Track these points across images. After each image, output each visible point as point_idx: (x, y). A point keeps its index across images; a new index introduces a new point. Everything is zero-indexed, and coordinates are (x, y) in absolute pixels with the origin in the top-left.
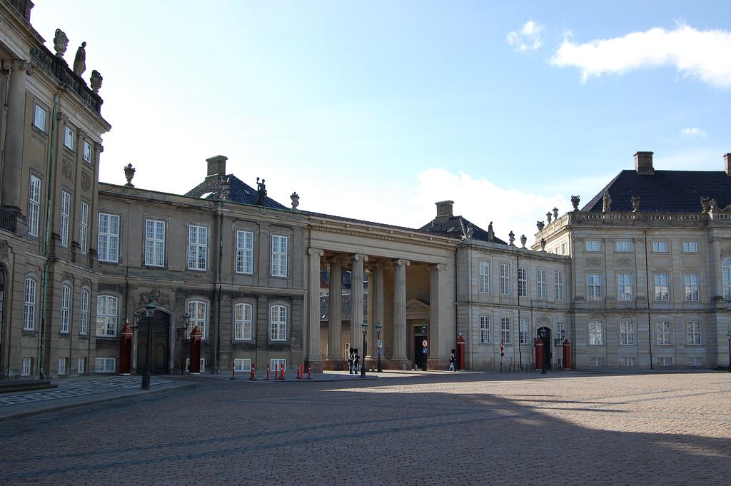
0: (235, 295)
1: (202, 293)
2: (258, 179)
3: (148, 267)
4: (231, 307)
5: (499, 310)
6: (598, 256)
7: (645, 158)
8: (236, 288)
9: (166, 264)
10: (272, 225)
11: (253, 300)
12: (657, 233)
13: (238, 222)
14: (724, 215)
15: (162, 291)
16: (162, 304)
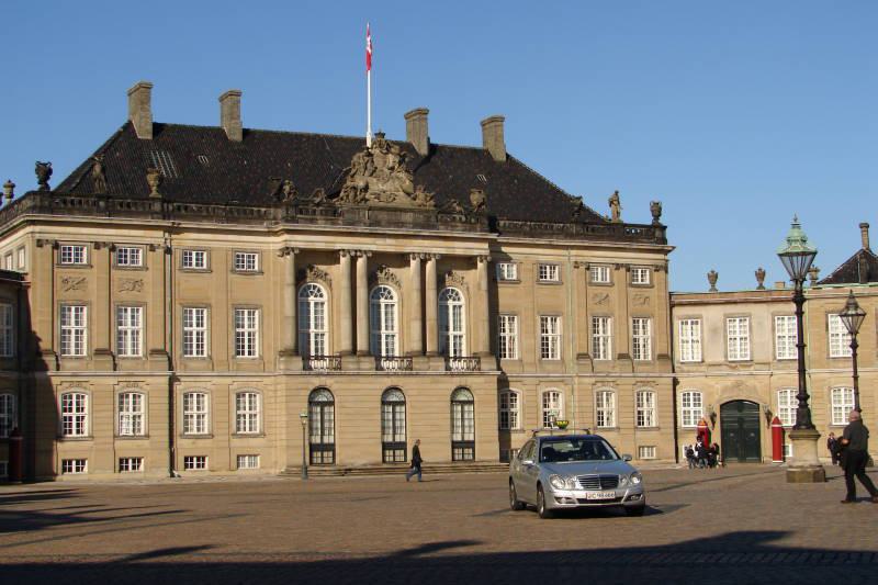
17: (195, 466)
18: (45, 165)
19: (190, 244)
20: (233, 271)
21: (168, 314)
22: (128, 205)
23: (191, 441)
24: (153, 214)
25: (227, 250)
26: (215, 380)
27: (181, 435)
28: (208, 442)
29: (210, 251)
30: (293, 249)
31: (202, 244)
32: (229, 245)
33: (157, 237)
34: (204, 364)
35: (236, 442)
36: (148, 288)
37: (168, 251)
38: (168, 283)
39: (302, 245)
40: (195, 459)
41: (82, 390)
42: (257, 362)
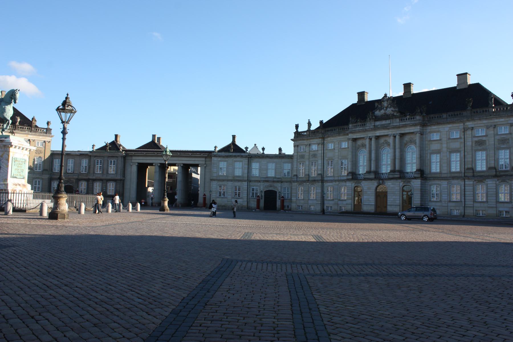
0: (95, 180)
1: (85, 180)
2: (105, 142)
3: (68, 173)
4: (93, 184)
5: (232, 182)
6: (304, 153)
7: (361, 95)
8: (94, 178)
9: (74, 172)
10: (109, 157)
11: (101, 181)
12: (329, 139)
13: (97, 157)
14: (355, 125)
15: (71, 179)
16: (71, 183)
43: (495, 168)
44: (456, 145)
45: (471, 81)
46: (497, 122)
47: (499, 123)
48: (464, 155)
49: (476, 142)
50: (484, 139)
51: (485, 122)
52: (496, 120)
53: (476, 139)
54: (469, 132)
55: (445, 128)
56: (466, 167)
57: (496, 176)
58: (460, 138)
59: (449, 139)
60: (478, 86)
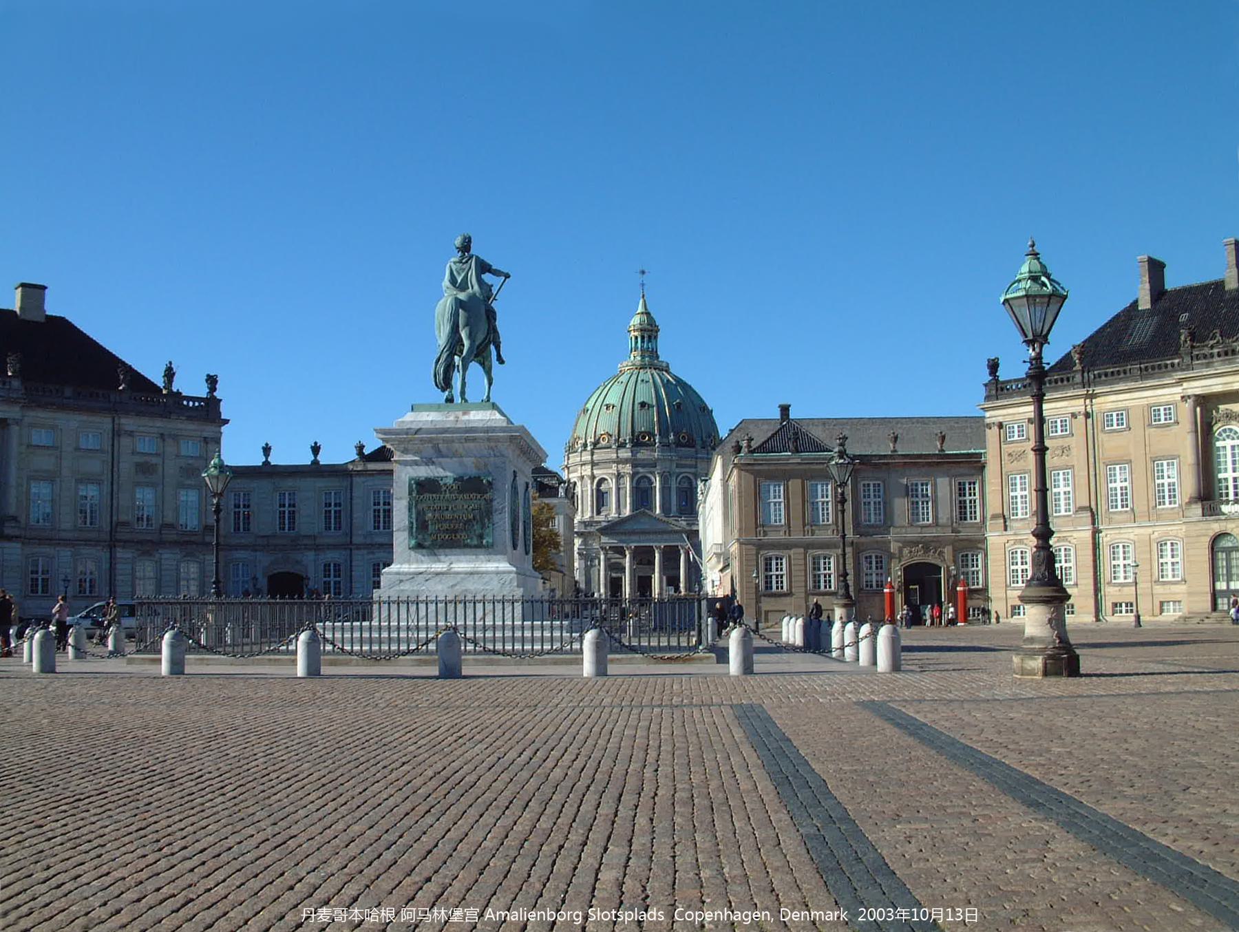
17: (1124, 611)
18: (993, 360)
19: (1110, 406)
20: (1150, 425)
21: (1092, 473)
22: (1056, 381)
23: (1117, 589)
24: (1074, 386)
25: (1143, 406)
26: (1137, 531)
27: (1108, 583)
28: (787, 600)
29: (1127, 409)
30: (1189, 397)
31: (1120, 405)
32: (1145, 402)
33: (1078, 405)
34: (1125, 516)
35: (1158, 589)
36: (1074, 451)
37: (1087, 415)
38: (1091, 444)
39: (1198, 392)
40: (1124, 605)
41: (1023, 546)
42: (1176, 510)
43: (171, 526)
44: (95, 466)
45: (53, 307)
46: (181, 429)
47: (184, 433)
48: (109, 490)
49: (138, 465)
50: (154, 460)
51: (159, 424)
52: (180, 426)
53: (138, 459)
54: (125, 441)
55: (70, 422)
56: (115, 518)
57: (175, 543)
58: (102, 451)
59: (77, 449)
60: (61, 326)
